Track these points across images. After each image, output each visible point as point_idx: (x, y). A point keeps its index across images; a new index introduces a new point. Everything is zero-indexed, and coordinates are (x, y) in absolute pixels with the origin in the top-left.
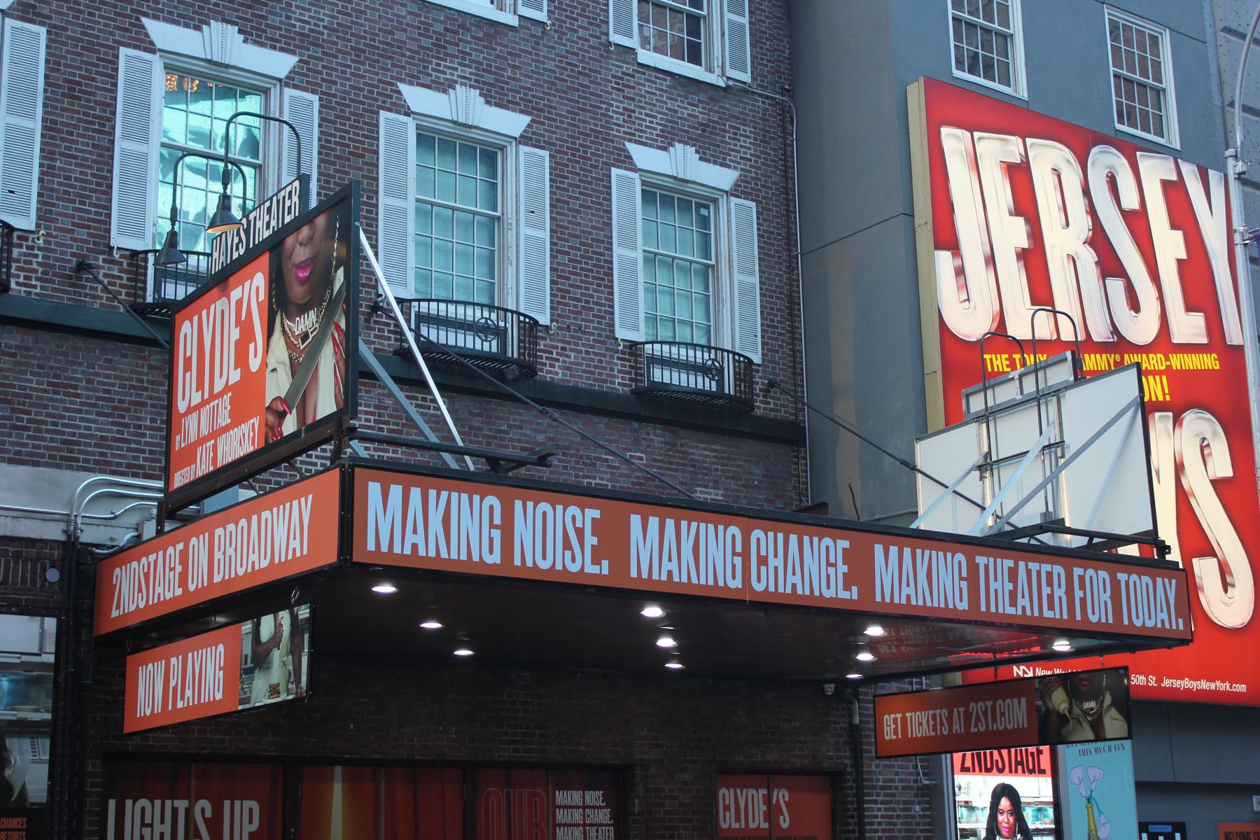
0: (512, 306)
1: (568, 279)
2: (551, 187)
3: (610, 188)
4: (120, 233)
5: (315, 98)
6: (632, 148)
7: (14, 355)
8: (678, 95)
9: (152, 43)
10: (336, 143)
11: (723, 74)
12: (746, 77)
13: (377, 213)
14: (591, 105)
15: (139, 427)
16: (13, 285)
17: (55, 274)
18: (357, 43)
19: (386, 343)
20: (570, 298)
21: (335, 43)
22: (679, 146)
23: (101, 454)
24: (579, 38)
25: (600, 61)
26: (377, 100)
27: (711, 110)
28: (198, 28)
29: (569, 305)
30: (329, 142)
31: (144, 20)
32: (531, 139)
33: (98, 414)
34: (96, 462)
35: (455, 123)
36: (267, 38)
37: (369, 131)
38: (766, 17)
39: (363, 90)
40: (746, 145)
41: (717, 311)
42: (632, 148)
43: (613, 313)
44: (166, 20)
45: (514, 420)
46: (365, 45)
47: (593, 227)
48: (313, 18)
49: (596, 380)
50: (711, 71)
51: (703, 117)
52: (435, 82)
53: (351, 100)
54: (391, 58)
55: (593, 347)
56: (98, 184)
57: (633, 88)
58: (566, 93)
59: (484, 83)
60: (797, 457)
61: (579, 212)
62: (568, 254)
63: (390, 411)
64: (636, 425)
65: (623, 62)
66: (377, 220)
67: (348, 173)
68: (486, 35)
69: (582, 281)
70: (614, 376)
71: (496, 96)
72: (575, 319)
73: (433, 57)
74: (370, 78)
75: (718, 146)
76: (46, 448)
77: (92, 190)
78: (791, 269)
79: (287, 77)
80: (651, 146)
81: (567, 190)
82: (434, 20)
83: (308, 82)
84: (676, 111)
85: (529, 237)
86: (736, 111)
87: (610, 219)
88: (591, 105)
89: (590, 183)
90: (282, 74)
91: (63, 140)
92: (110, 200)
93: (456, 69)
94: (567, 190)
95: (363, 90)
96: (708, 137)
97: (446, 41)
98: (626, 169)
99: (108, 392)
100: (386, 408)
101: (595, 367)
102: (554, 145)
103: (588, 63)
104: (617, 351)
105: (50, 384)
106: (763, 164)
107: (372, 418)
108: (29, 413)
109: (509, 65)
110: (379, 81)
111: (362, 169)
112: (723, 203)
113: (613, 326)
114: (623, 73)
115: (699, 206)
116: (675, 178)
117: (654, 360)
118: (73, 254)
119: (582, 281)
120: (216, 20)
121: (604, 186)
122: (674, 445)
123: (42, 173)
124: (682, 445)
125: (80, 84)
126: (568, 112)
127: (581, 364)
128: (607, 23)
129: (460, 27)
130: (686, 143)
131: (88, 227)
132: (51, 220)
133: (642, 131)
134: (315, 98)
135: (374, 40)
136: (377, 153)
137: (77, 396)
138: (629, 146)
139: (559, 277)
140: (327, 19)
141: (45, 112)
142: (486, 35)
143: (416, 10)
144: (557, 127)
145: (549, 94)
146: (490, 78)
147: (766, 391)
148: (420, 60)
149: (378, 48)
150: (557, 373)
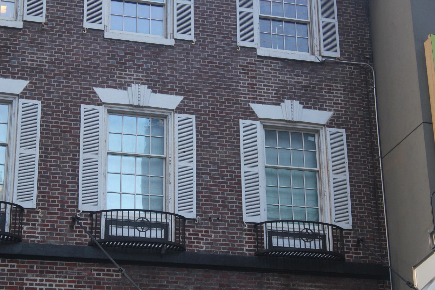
0: (171, 211)
1: (210, 189)
2: (197, 135)
3: (239, 132)
5: (39, 103)
6: (255, 107)
8: (287, 71)
10: (52, 126)
11: (320, 55)
12: (337, 54)
13: (79, 164)
14: (225, 85)
18: (67, 68)
19: (83, 239)
20: (211, 201)
21: (53, 70)
22: (287, 102)
24: (217, 46)
25: (231, 58)
26: (80, 99)
27: (311, 77)
29: (210, 205)
30: (49, 126)
32: (184, 109)
35: (132, 106)
36: (9, 73)
37: (74, 117)
38: (350, 17)
39: (71, 94)
40: (338, 94)
41: (321, 199)
42: (255, 107)
43: (241, 207)
45: (171, 278)
46: (72, 69)
47: (227, 157)
48: (39, 58)
49: (229, 249)
50: (313, 54)
51: (303, 81)
52: (118, 84)
53: (63, 101)
54: (89, 74)
55: (228, 229)
57: (255, 71)
58: (208, 80)
59: (151, 81)
60: (383, 287)
61: (217, 148)
62: (209, 174)
63: (86, 279)
64: (259, 275)
65: (248, 57)
66: (78, 167)
67: (61, 143)
68: (153, 53)
69: (219, 190)
70: (244, 246)
71: (158, 87)
72: (214, 213)
73: (117, 70)
74: (75, 87)
75: (317, 98)
78: (375, 167)
79: (22, 93)
80: (268, 104)
81: (209, 136)
82: (118, 49)
83: (35, 94)
84: (286, 81)
85: (183, 166)
86: (329, 75)
87: (239, 150)
88: (225, 85)
89: (225, 131)
90: (18, 92)
93: (133, 75)
94: (209, 136)
95: (71, 94)
96: (310, 94)
97: (125, 60)
98: (250, 119)
100: (83, 278)
101: (229, 241)
102: (200, 111)
103: (223, 61)
104: (245, 230)
106: (351, 105)
107: (73, 284)
109: (169, 68)
110: (81, 88)
111: (69, 140)
112: (322, 132)
113: (242, 215)
114: (247, 63)
115: (307, 135)
116: (286, 121)
117: (272, 234)
119: (219, 190)
121: (234, 131)
122: (288, 285)
124: (294, 285)
126: (209, 90)
127: (220, 240)
128: (236, 35)
129: (135, 51)
130: (292, 99)
133: (262, 96)
134: (39, 103)
135: (79, 66)
136: (79, 129)
138: (252, 105)
139: (203, 188)
140: (48, 57)
142: (153, 53)
143: (107, 45)
144: (201, 100)
145: (196, 82)
146: (155, 77)
147: (357, 246)
148: (108, 73)
149: (81, 70)
150: (202, 247)
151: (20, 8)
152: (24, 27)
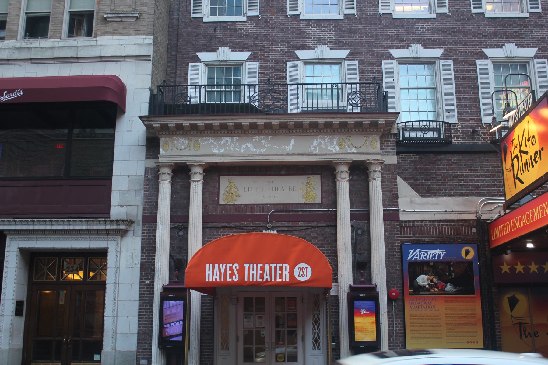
4: (485, 119)
7: (457, 163)
9: (487, 56)
15: (499, 180)
16: (453, 141)
17: (466, 135)
23: (488, 190)
28: (501, 47)
31: (483, 49)
33: (486, 177)
34: (487, 193)
44: (490, 48)
56: (476, 105)
76: (470, 190)
77: (474, 107)
90: (533, 55)
91: (462, 93)
92: (480, 109)
99: (488, 170)
105: (469, 170)
108: (463, 180)
118: (471, 128)
120: (507, 43)
123: (457, 105)
125: (465, 74)
131: (474, 119)
132: (462, 119)
137: (478, 172)
141: (456, 86)
151: (525, 5)
152: (530, 16)
